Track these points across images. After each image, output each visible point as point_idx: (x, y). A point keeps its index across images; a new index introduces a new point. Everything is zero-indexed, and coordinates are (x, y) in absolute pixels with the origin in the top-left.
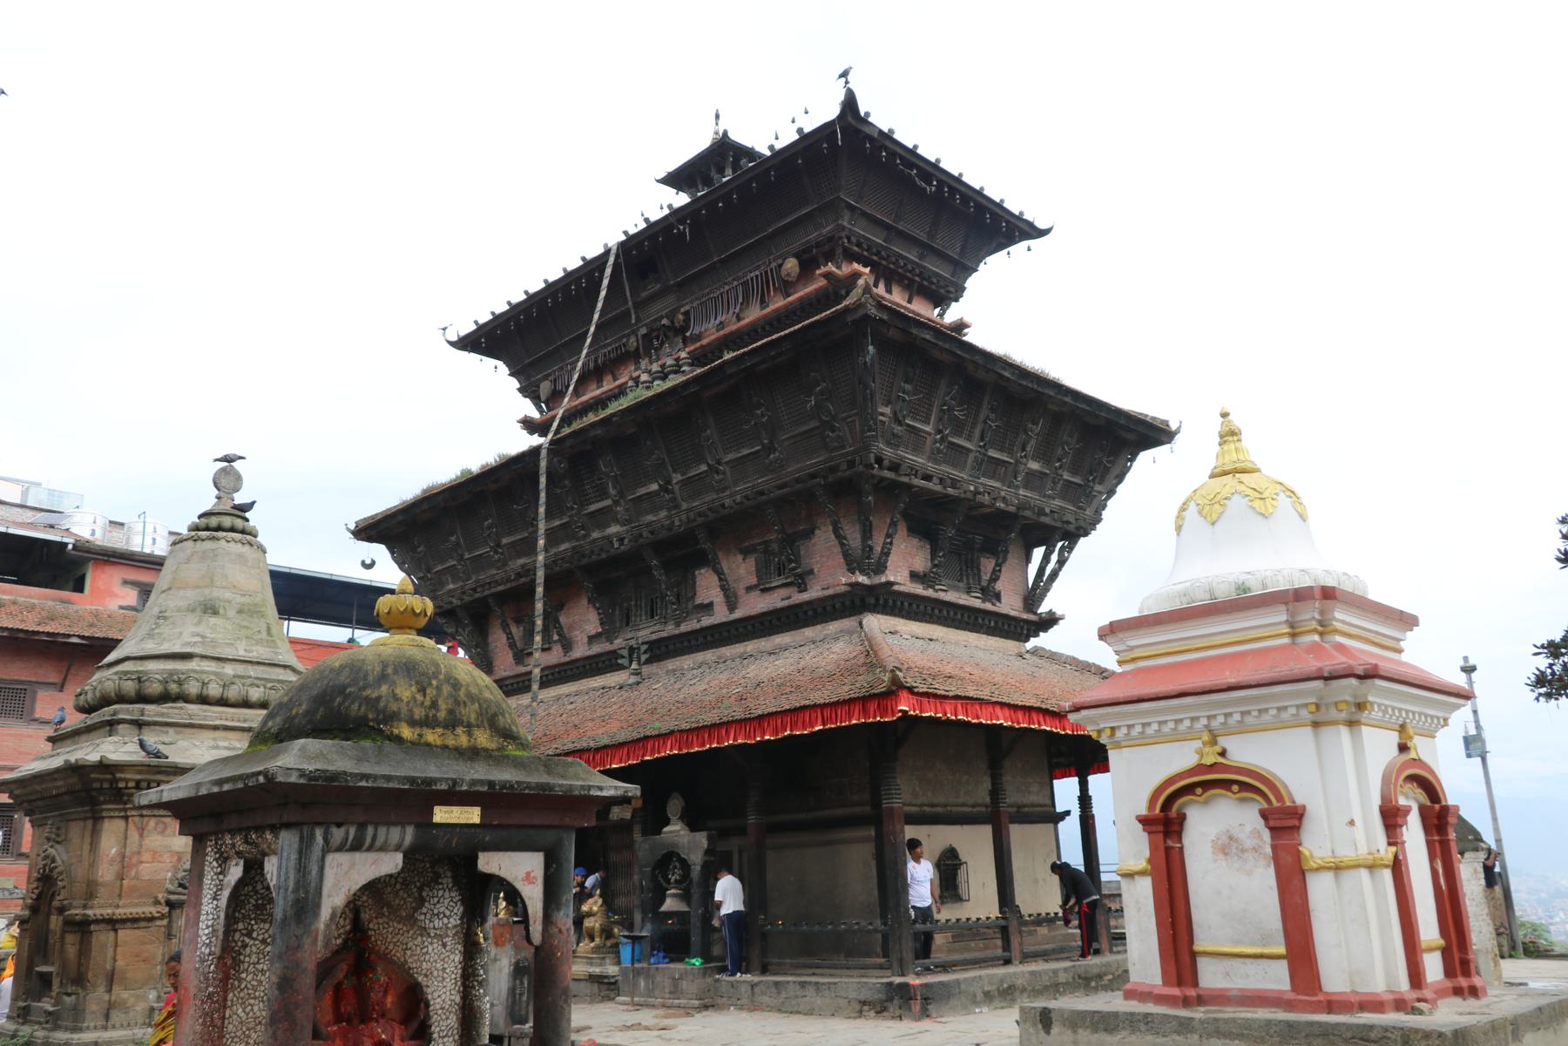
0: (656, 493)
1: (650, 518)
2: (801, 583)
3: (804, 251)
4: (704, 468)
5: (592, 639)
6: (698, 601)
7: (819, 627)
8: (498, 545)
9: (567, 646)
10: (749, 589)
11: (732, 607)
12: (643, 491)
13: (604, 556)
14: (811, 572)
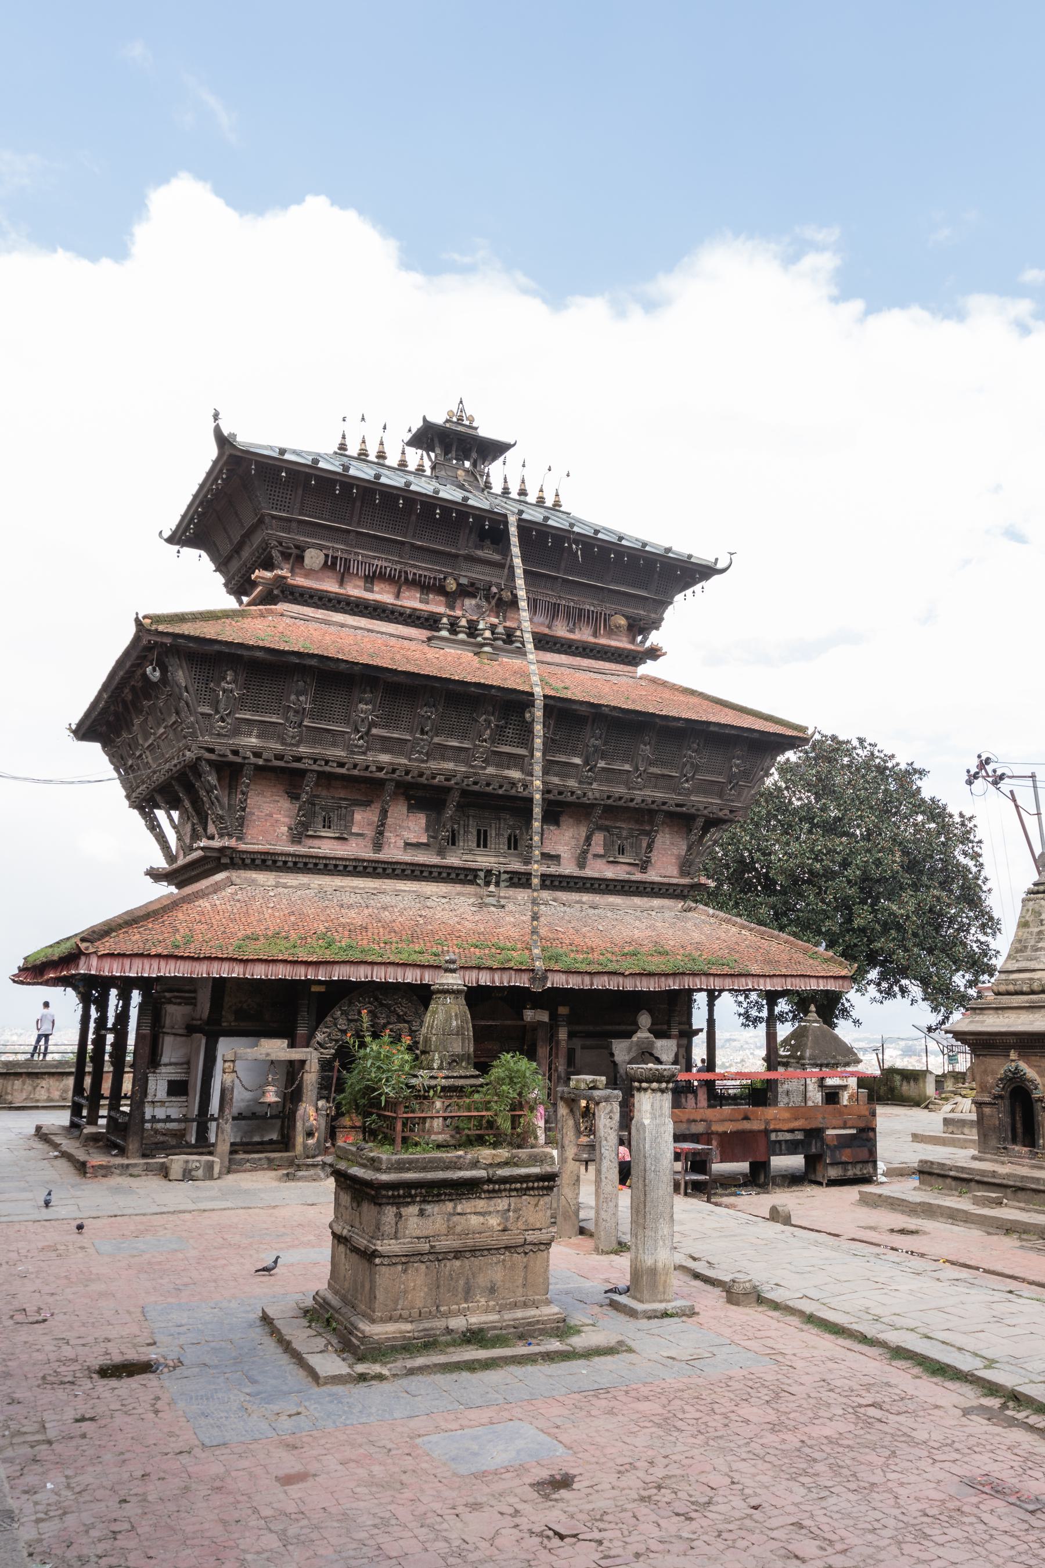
0: (577, 765)
1: (556, 780)
2: (644, 866)
4: (627, 767)
5: (408, 845)
7: (645, 899)
8: (369, 730)
9: (378, 846)
10: (596, 856)
11: (582, 865)
12: (563, 759)
13: (501, 792)
14: (650, 861)
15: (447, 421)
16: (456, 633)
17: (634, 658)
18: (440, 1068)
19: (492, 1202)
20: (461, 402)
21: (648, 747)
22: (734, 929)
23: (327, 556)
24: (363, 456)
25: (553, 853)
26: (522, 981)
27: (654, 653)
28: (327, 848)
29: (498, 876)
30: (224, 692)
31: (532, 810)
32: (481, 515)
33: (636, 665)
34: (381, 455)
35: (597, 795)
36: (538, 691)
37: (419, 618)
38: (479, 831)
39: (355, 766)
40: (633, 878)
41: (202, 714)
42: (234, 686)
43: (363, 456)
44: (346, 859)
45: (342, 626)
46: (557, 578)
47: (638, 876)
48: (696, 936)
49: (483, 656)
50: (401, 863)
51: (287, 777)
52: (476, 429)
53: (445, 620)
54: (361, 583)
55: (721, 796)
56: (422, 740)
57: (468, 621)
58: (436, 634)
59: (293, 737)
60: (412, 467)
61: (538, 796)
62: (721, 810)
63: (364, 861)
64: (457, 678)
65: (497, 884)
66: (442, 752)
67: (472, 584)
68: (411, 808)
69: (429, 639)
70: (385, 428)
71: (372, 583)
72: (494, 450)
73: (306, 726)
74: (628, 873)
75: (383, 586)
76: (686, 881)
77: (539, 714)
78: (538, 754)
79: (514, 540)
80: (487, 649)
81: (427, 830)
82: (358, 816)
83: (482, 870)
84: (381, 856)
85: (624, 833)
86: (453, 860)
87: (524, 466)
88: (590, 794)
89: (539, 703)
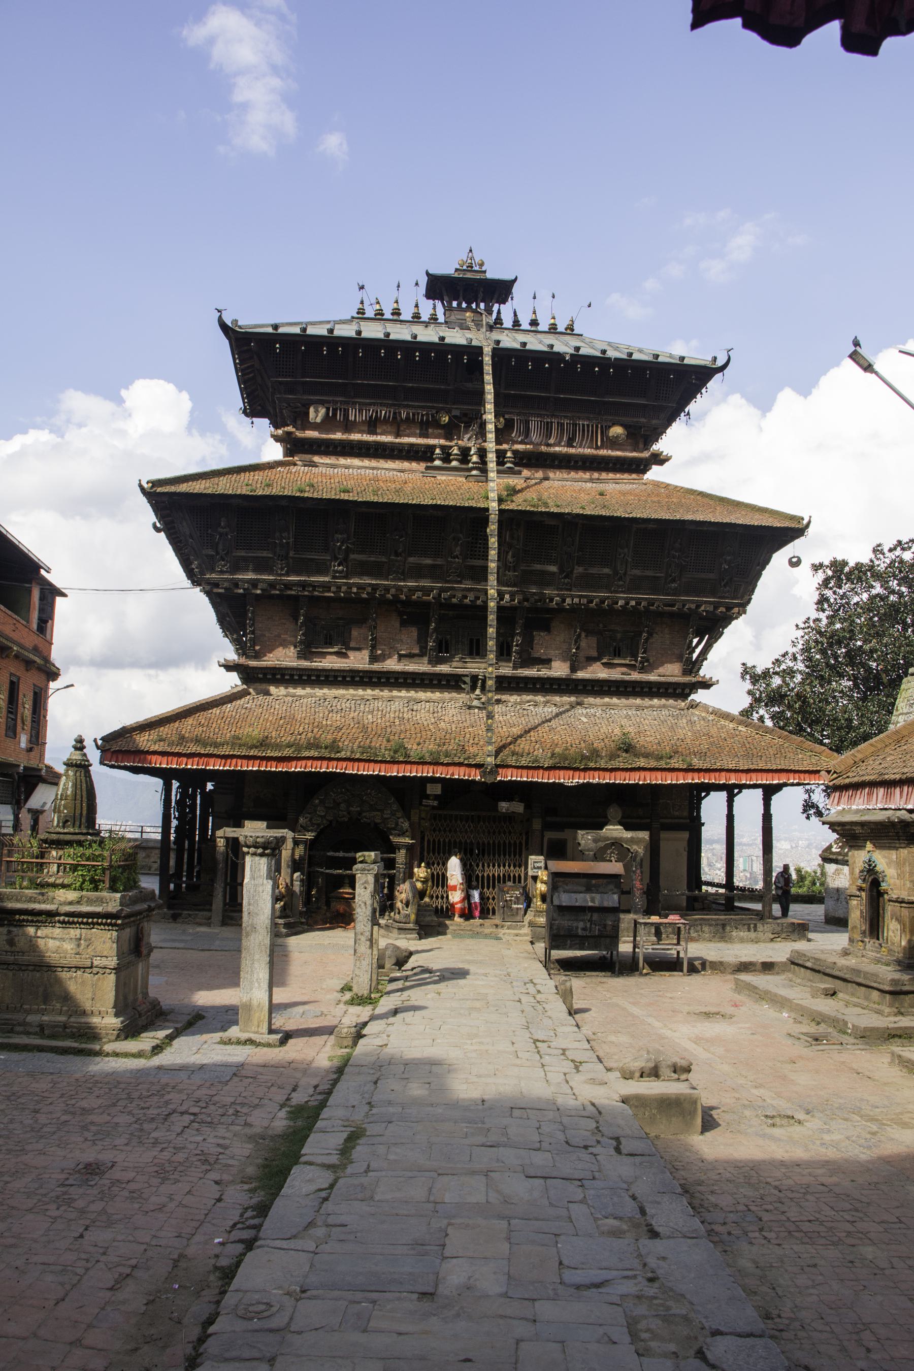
0: (553, 574)
3: (630, 426)
6: (536, 655)
12: (538, 567)
15: (457, 270)
16: (450, 461)
17: (638, 466)
18: (58, 826)
19: (66, 931)
20: (471, 251)
21: (626, 550)
22: (731, 725)
23: (328, 409)
24: (380, 313)
25: (545, 657)
26: (476, 776)
27: (659, 459)
28: (330, 662)
29: (484, 682)
30: (221, 536)
31: (498, 619)
32: (457, 350)
33: (644, 471)
34: (396, 312)
35: (576, 600)
36: (494, 506)
37: (417, 452)
38: (471, 641)
39: (339, 587)
40: (626, 678)
41: (206, 556)
42: (227, 530)
43: (380, 313)
44: (344, 671)
45: (347, 467)
46: (549, 398)
47: (635, 676)
48: (681, 733)
49: (471, 479)
50: (394, 672)
51: (288, 603)
52: (485, 272)
53: (438, 451)
54: (366, 428)
55: (713, 594)
56: (396, 561)
57: (460, 448)
58: (429, 464)
59: (282, 569)
60: (425, 317)
61: (492, 604)
62: (716, 608)
63: (358, 671)
64: (414, 502)
65: (483, 689)
66: (418, 572)
67: (465, 415)
68: (404, 624)
69: (427, 468)
70: (399, 286)
71: (375, 427)
72: (500, 290)
73: (292, 558)
74: (623, 674)
75: (385, 427)
76: (687, 679)
77: (493, 528)
78: (493, 565)
79: (488, 369)
80: (474, 472)
81: (419, 641)
82: (355, 633)
83: (467, 676)
84: (376, 667)
85: (619, 636)
86: (444, 668)
87: (535, 298)
88: (568, 601)
89: (494, 517)
